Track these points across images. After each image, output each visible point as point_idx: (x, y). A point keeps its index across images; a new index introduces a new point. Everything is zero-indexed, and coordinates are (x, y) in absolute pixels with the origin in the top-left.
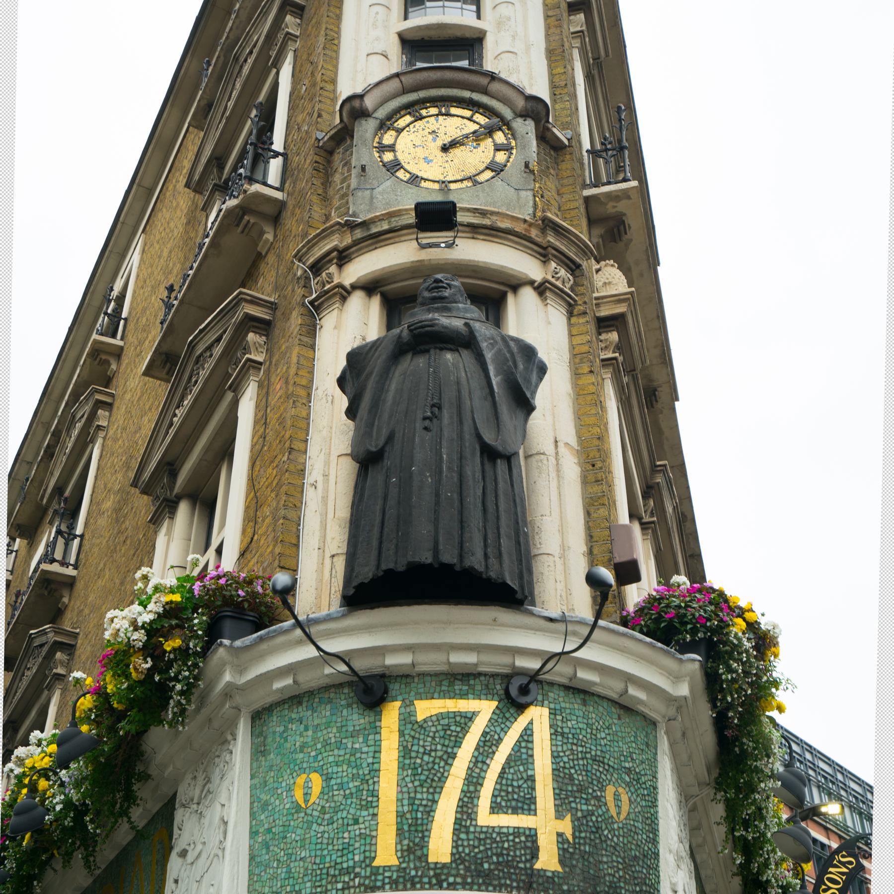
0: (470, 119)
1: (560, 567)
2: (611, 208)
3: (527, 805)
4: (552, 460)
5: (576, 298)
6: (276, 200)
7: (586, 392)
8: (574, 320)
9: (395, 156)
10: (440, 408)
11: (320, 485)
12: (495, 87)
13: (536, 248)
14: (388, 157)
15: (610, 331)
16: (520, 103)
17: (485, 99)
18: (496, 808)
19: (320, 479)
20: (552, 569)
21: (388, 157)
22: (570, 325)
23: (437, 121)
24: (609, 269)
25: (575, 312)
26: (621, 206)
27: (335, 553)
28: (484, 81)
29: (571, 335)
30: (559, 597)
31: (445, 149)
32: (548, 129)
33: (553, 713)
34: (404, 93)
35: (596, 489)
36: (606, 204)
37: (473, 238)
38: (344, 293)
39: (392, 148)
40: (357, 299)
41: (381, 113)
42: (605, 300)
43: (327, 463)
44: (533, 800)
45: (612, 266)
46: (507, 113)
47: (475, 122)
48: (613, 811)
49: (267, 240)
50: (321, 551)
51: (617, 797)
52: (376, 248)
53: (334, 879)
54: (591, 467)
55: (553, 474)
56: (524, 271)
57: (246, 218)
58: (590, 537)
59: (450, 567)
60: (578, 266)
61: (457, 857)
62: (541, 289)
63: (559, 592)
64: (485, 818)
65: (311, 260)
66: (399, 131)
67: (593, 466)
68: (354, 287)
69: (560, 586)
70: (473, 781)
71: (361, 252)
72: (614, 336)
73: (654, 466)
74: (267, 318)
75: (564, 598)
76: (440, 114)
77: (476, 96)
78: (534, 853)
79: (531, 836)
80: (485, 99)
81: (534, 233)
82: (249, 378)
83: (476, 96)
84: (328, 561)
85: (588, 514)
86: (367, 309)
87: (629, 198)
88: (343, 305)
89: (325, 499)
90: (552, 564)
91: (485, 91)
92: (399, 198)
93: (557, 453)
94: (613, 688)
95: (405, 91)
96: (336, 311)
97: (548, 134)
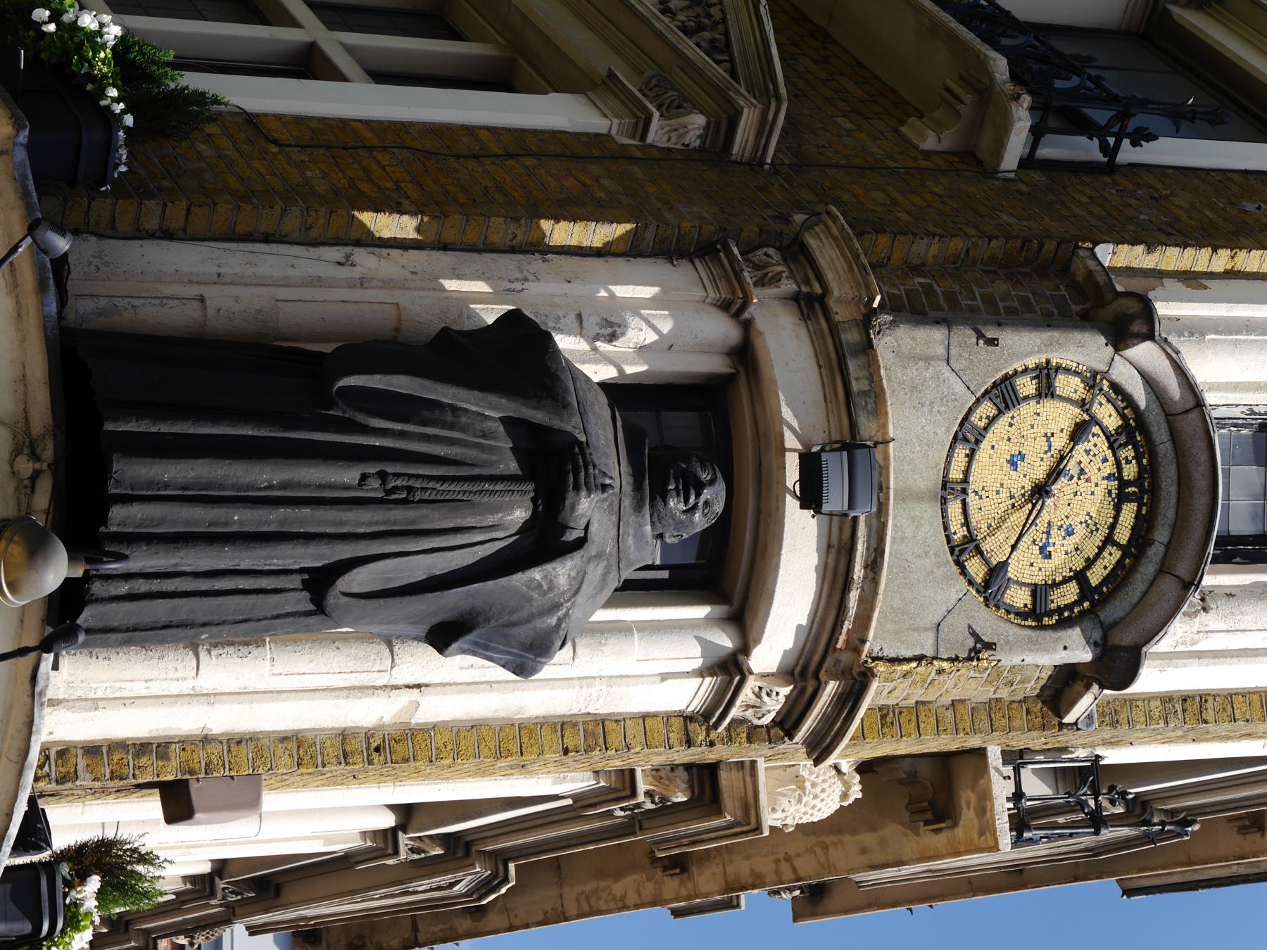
0: (1109, 540)
1: (175, 688)
2: (966, 797)
4: (383, 680)
5: (720, 729)
6: (999, 157)
7: (525, 740)
8: (677, 723)
9: (1026, 398)
10: (404, 502)
11: (345, 272)
12: (1168, 586)
13: (816, 658)
14: (1027, 386)
15: (691, 787)
16: (1124, 638)
17: (1148, 568)
19: (356, 273)
20: (171, 674)
21: (1027, 386)
22: (668, 716)
23: (1108, 478)
24: (838, 787)
25: (692, 727)
26: (968, 816)
27: (208, 303)
28: (1183, 570)
29: (644, 717)
30: (118, 685)
32: (1088, 687)
34: (1168, 415)
35: (333, 751)
36: (973, 790)
37: (829, 546)
38: (734, 307)
39: (1046, 391)
40: (721, 329)
42: (748, 779)
43: (387, 284)
45: (844, 796)
47: (1101, 549)
49: (924, 139)
50: (215, 278)
52: (820, 367)
54: (374, 745)
55: (354, 680)
56: (766, 636)
57: (968, 98)
58: (236, 741)
59: (104, 521)
60: (790, 734)
63: (128, 685)
65: (812, 242)
67: (377, 750)
69: (139, 689)
71: (815, 337)
73: (503, 858)
74: (735, 150)
75: (117, 695)
76: (1123, 484)
77: (1155, 553)
82: (617, 116)
84: (194, 290)
85: (284, 738)
86: (705, 349)
87: (982, 833)
88: (715, 305)
89: (317, 282)
90: (179, 675)
91: (1163, 569)
92: (926, 409)
93: (396, 687)
96: (702, 293)
97: (1079, 686)
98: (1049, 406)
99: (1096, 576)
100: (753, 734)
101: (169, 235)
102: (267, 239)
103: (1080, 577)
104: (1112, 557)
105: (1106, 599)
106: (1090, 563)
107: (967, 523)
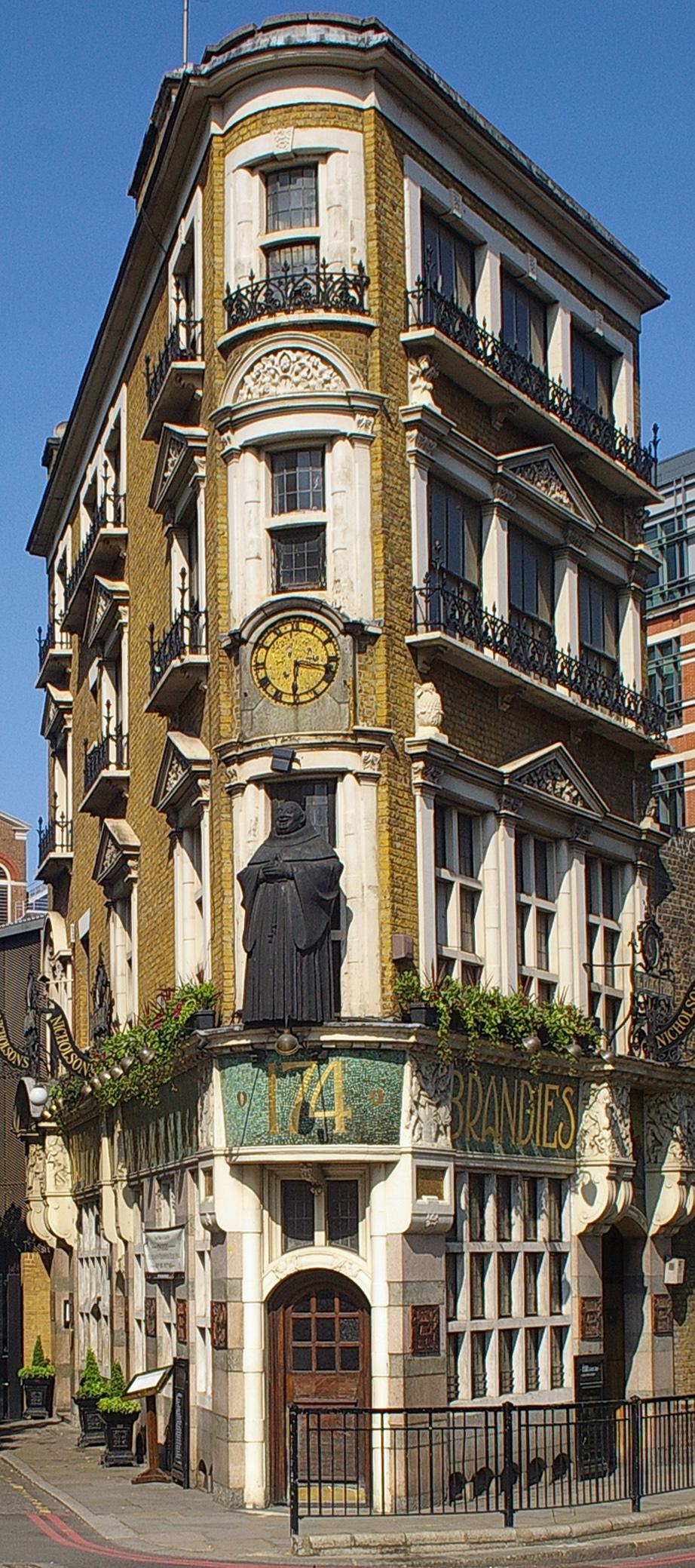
0: (312, 633)
12: (323, 610)
16: (341, 627)
17: (320, 617)
21: (262, 674)
22: (378, 792)
39: (263, 665)
41: (253, 638)
44: (333, 1105)
46: (336, 632)
53: (254, 1139)
62: (359, 777)
66: (267, 649)
68: (249, 782)
77: (314, 615)
78: (334, 1128)
79: (333, 1120)
80: (320, 617)
83: (314, 615)
91: (319, 612)
95: (267, 617)
98: (268, 666)
99: (324, 637)
101: (234, 976)
102: (233, 945)
103: (325, 643)
104: (318, 631)
105: (331, 633)
106: (320, 640)
107: (307, 693)
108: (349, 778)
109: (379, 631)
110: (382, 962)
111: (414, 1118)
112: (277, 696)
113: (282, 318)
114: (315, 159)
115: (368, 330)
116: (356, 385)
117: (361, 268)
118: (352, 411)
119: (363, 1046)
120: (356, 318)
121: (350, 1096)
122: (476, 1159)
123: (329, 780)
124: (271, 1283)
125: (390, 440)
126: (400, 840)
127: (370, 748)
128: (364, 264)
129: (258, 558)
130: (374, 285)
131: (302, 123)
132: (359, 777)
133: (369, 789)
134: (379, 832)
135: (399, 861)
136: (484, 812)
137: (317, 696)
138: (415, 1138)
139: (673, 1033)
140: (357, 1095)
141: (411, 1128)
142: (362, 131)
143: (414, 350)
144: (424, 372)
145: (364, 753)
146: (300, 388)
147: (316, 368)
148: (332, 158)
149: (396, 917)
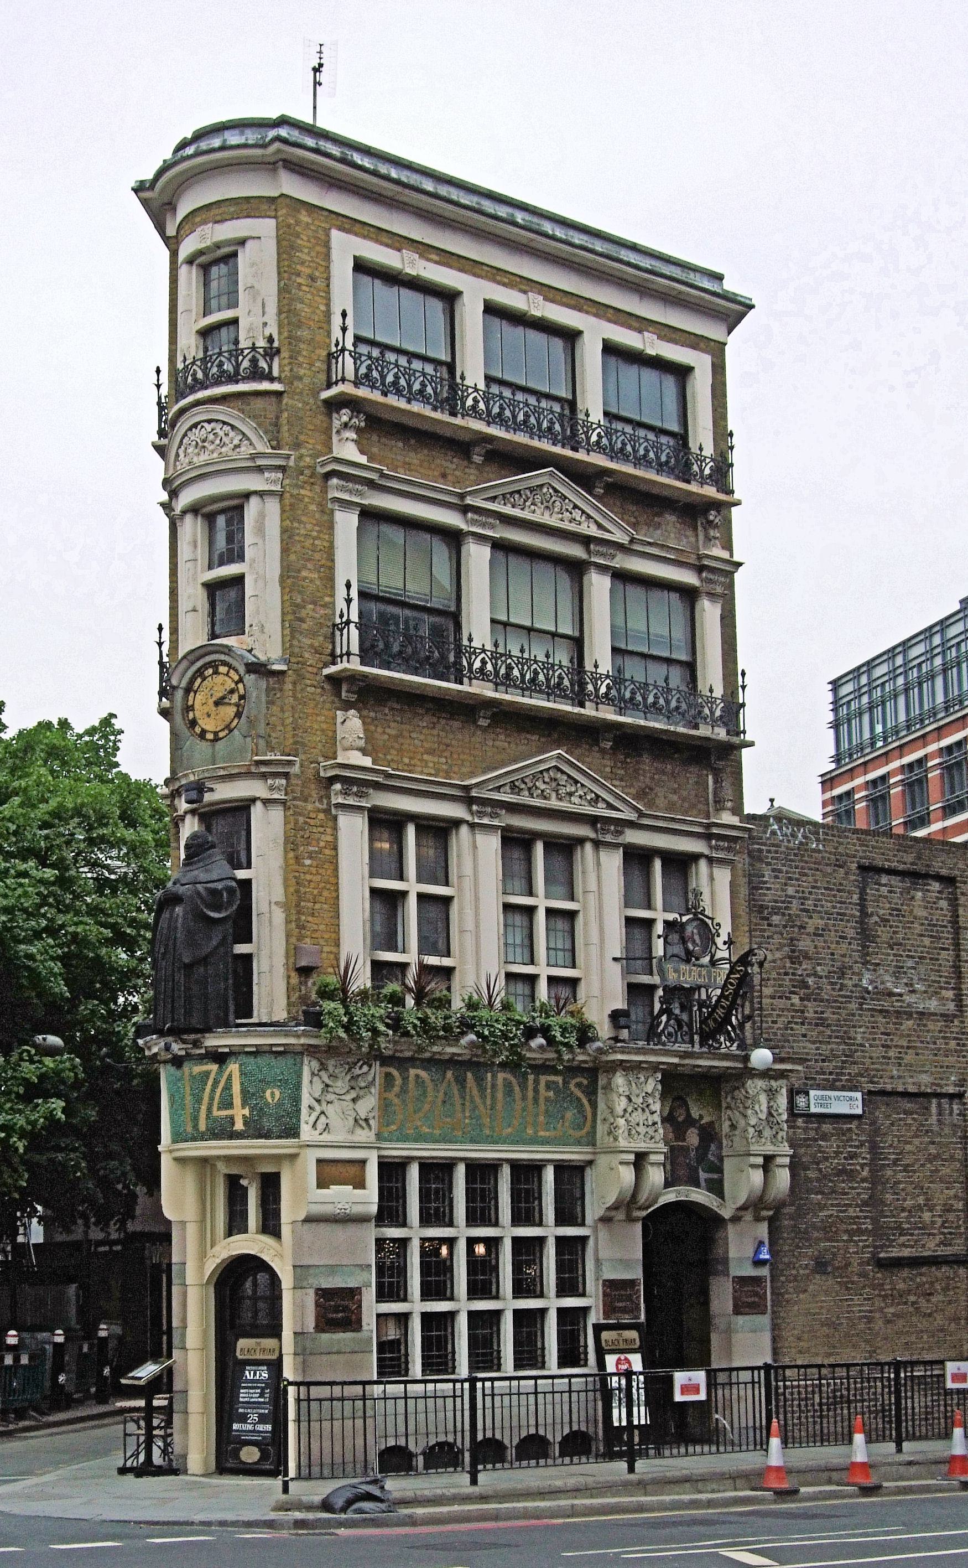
0: (227, 675)
3: (230, 1105)
18: (219, 1109)
31: (217, 704)
33: (241, 1065)
39: (191, 708)
40: (188, 818)
41: (184, 684)
48: (270, 1100)
51: (273, 1094)
61: (207, 1129)
64: (216, 1113)
66: (195, 692)
68: (186, 813)
70: (212, 1099)
72: (338, 786)
78: (233, 1124)
81: (253, 769)
94: (267, 1048)
98: (196, 707)
100: (287, 786)
104: (232, 673)
108: (259, 804)
109: (284, 668)
110: (288, 969)
111: (314, 1115)
112: (203, 735)
113: (201, 395)
114: (232, 249)
115: (279, 394)
116: (262, 447)
117: (270, 340)
118: (260, 469)
119: (282, 1049)
120: (265, 386)
121: (246, 1096)
122: (396, 1151)
123: (242, 808)
124: (211, 1265)
125: (302, 492)
126: (310, 858)
127: (276, 775)
128: (275, 336)
129: (194, 610)
130: (285, 354)
131: (218, 218)
132: (266, 802)
133: (277, 814)
134: (286, 852)
135: (308, 877)
136: (456, 823)
137: (231, 731)
138: (318, 1132)
139: (715, 1020)
140: (253, 1094)
141: (311, 1123)
142: (275, 217)
143: (333, 405)
144: (346, 425)
145: (270, 781)
146: (215, 455)
147: (226, 435)
148: (249, 244)
149: (304, 927)
